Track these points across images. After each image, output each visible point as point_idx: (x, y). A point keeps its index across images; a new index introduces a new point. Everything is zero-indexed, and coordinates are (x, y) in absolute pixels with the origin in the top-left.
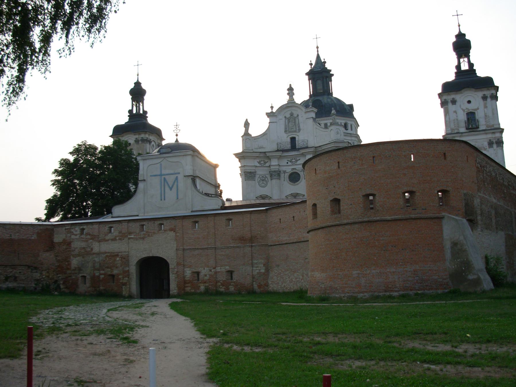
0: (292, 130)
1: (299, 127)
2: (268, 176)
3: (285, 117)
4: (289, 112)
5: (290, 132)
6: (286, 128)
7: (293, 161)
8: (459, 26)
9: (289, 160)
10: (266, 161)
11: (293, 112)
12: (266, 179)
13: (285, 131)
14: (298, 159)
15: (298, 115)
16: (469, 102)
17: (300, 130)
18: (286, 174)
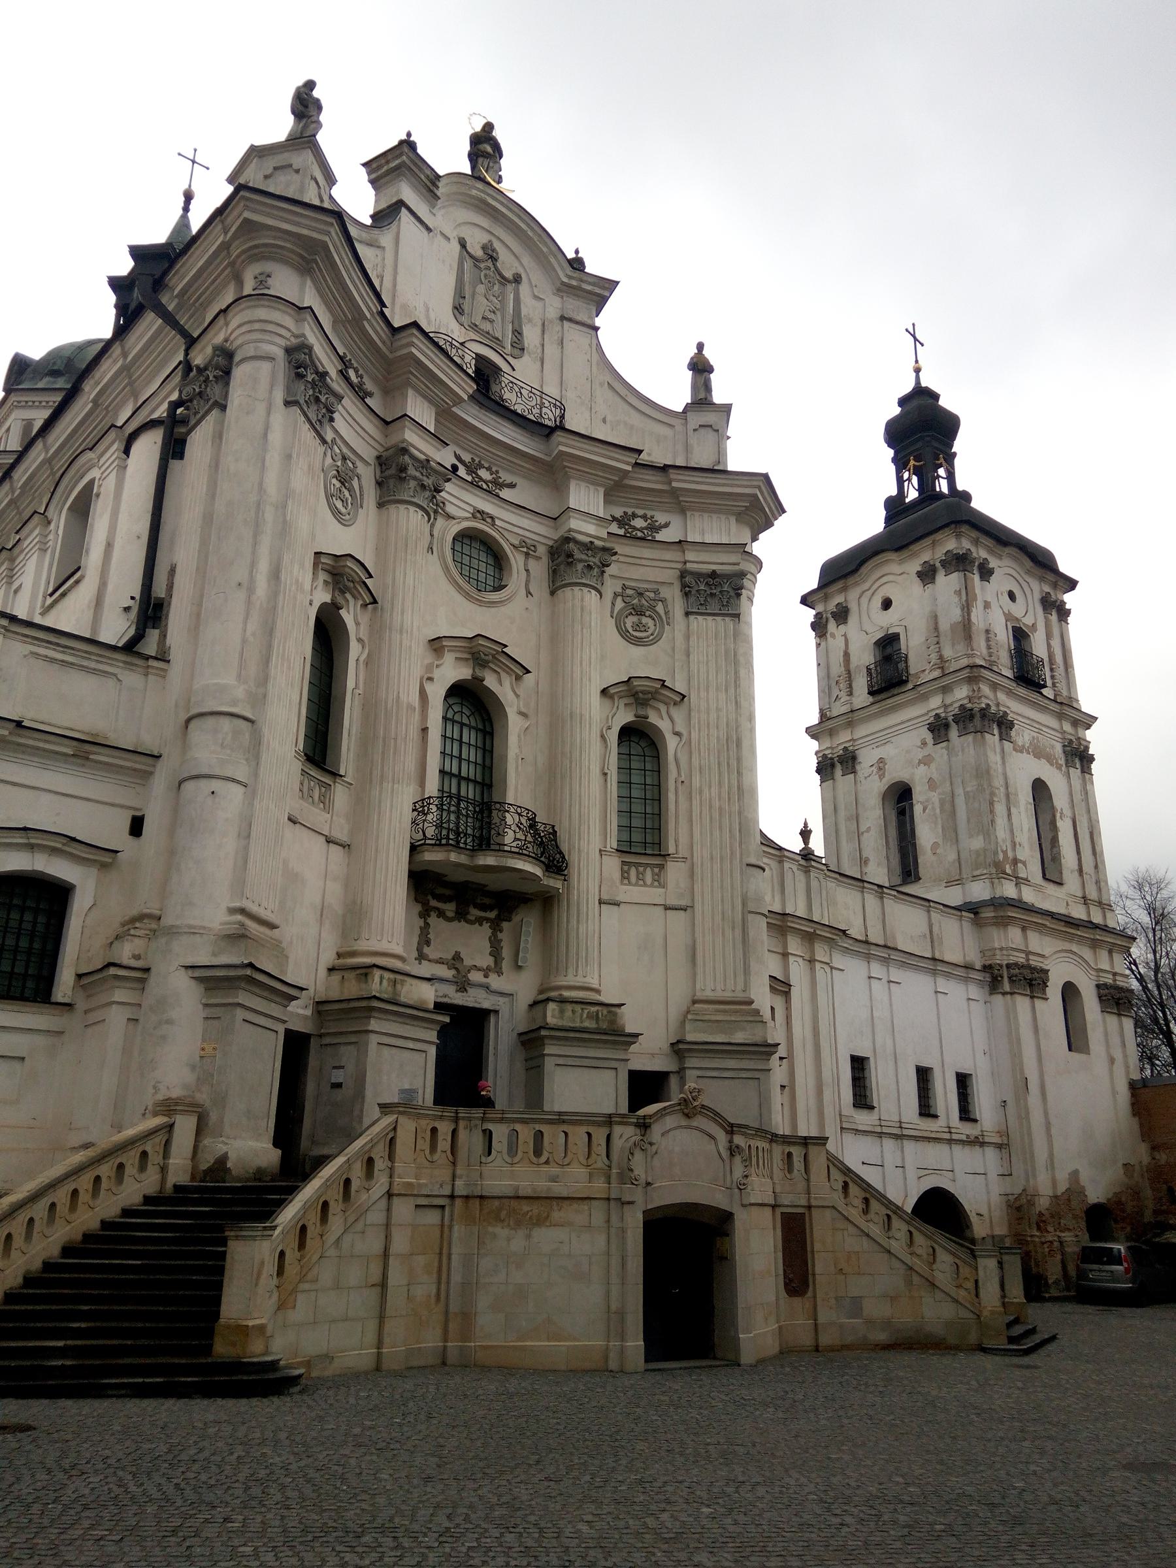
0: (486, 326)
1: (518, 333)
2: (367, 475)
3: (463, 244)
4: (485, 238)
5: (474, 327)
6: (460, 294)
7: (484, 474)
8: (917, 371)
9: (467, 457)
10: (369, 386)
11: (497, 245)
12: (355, 483)
13: (458, 309)
14: (505, 477)
15: (517, 279)
16: (1012, 596)
17: (519, 348)
18: (440, 522)
